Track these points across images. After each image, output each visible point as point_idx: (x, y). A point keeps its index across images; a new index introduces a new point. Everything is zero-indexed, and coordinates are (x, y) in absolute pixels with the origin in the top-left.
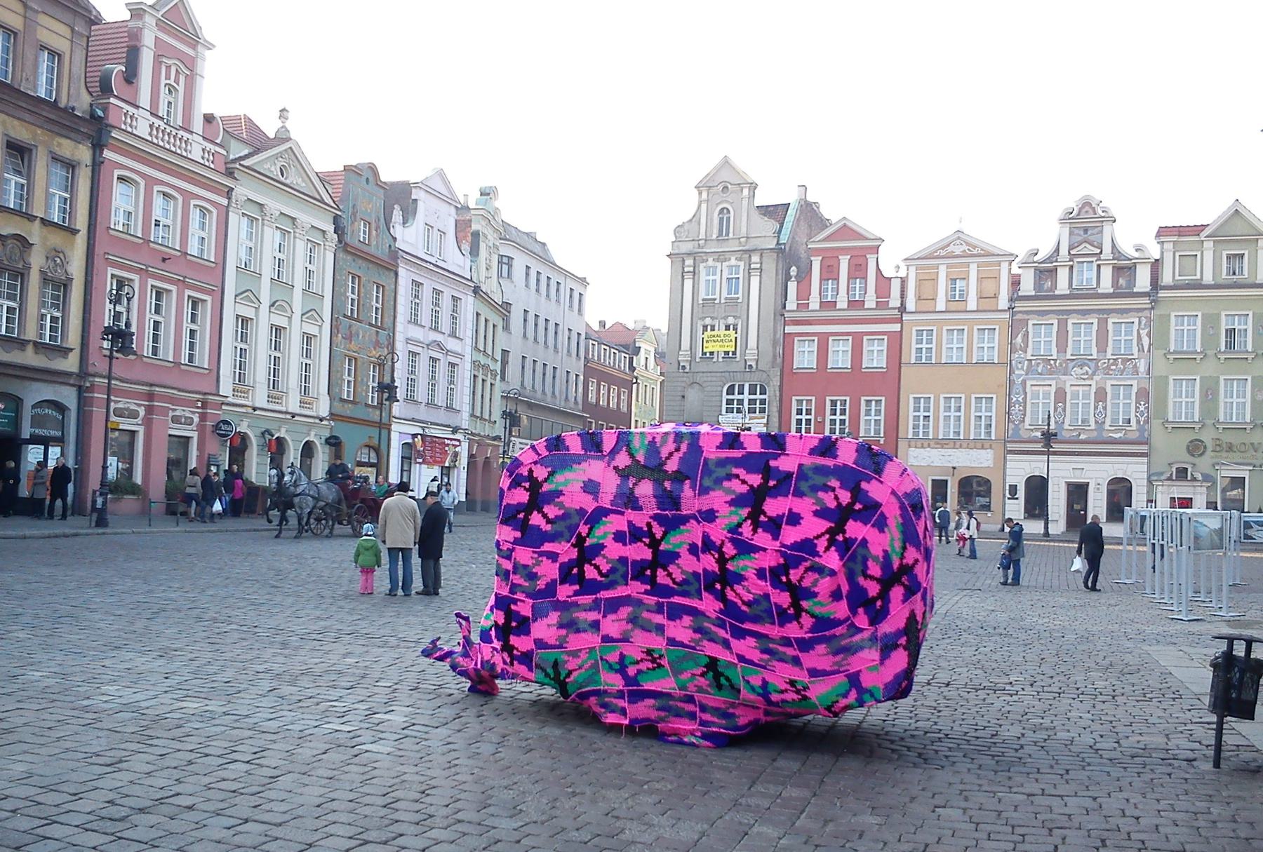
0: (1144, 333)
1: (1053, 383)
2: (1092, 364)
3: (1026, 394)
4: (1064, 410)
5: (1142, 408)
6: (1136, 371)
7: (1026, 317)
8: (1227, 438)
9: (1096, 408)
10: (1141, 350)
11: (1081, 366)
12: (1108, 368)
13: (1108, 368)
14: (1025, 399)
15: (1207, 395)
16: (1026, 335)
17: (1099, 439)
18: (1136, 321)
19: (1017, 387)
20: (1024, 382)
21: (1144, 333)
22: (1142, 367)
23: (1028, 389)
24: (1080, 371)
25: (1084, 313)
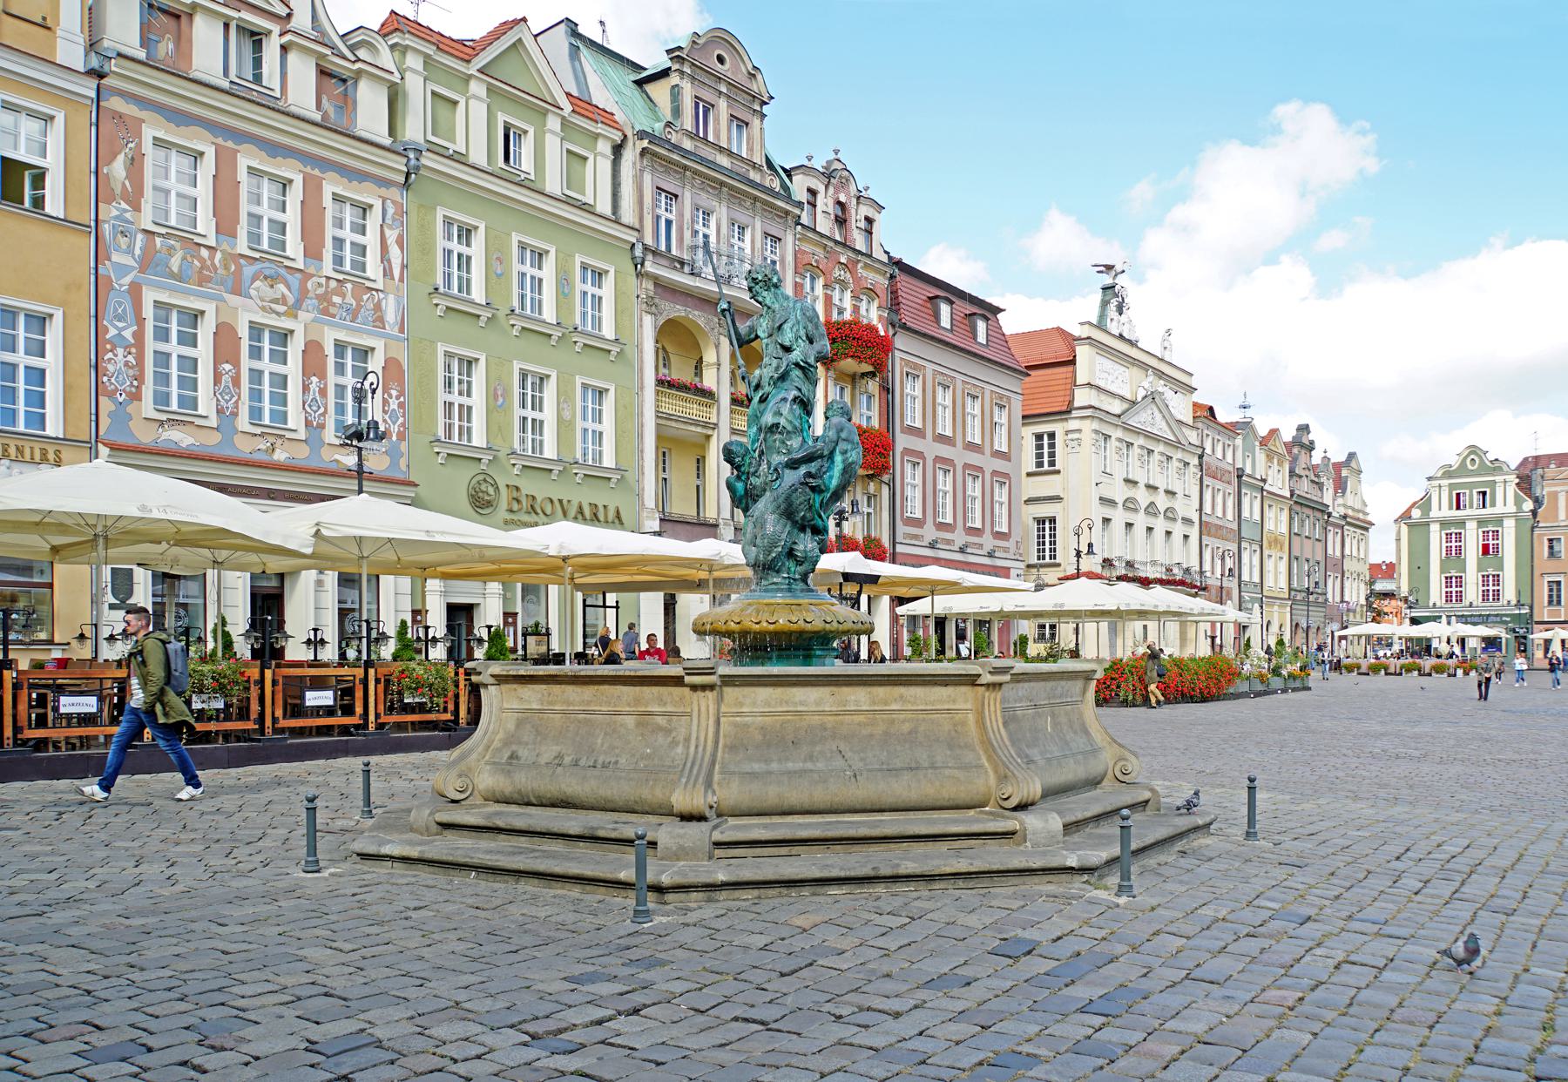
0: (392, 236)
1: (209, 308)
2: (294, 280)
3: (140, 321)
4: (236, 381)
5: (394, 404)
6: (380, 321)
7: (130, 110)
8: (529, 486)
9: (306, 388)
10: (388, 273)
11: (272, 280)
12: (325, 298)
13: (325, 298)
14: (139, 336)
15: (496, 397)
16: (136, 163)
17: (314, 464)
18: (378, 204)
19: (117, 302)
20: (135, 291)
21: (392, 236)
22: (391, 316)
23: (148, 312)
24: (269, 293)
25: (274, 150)
